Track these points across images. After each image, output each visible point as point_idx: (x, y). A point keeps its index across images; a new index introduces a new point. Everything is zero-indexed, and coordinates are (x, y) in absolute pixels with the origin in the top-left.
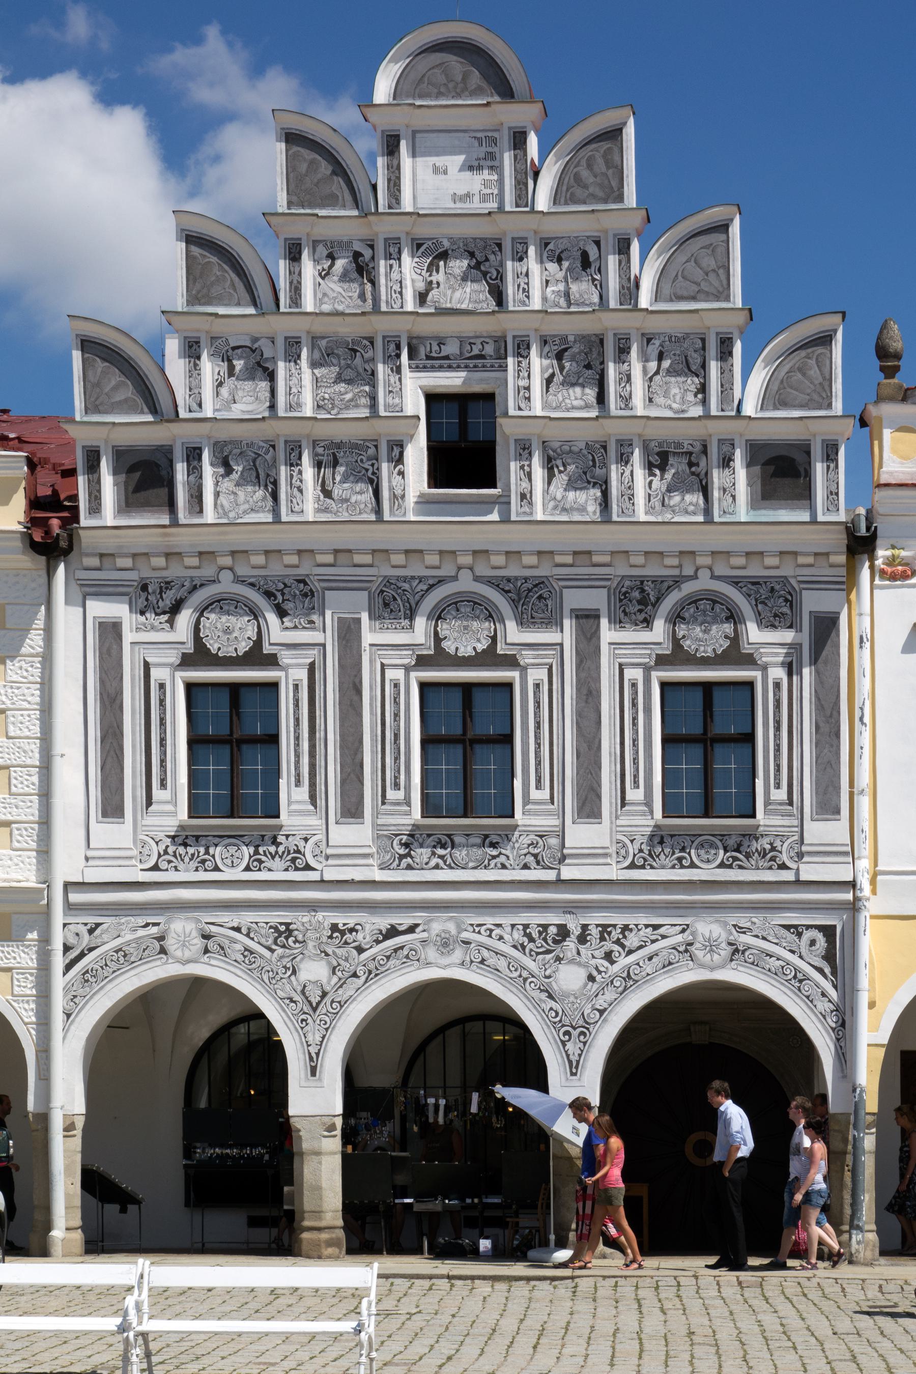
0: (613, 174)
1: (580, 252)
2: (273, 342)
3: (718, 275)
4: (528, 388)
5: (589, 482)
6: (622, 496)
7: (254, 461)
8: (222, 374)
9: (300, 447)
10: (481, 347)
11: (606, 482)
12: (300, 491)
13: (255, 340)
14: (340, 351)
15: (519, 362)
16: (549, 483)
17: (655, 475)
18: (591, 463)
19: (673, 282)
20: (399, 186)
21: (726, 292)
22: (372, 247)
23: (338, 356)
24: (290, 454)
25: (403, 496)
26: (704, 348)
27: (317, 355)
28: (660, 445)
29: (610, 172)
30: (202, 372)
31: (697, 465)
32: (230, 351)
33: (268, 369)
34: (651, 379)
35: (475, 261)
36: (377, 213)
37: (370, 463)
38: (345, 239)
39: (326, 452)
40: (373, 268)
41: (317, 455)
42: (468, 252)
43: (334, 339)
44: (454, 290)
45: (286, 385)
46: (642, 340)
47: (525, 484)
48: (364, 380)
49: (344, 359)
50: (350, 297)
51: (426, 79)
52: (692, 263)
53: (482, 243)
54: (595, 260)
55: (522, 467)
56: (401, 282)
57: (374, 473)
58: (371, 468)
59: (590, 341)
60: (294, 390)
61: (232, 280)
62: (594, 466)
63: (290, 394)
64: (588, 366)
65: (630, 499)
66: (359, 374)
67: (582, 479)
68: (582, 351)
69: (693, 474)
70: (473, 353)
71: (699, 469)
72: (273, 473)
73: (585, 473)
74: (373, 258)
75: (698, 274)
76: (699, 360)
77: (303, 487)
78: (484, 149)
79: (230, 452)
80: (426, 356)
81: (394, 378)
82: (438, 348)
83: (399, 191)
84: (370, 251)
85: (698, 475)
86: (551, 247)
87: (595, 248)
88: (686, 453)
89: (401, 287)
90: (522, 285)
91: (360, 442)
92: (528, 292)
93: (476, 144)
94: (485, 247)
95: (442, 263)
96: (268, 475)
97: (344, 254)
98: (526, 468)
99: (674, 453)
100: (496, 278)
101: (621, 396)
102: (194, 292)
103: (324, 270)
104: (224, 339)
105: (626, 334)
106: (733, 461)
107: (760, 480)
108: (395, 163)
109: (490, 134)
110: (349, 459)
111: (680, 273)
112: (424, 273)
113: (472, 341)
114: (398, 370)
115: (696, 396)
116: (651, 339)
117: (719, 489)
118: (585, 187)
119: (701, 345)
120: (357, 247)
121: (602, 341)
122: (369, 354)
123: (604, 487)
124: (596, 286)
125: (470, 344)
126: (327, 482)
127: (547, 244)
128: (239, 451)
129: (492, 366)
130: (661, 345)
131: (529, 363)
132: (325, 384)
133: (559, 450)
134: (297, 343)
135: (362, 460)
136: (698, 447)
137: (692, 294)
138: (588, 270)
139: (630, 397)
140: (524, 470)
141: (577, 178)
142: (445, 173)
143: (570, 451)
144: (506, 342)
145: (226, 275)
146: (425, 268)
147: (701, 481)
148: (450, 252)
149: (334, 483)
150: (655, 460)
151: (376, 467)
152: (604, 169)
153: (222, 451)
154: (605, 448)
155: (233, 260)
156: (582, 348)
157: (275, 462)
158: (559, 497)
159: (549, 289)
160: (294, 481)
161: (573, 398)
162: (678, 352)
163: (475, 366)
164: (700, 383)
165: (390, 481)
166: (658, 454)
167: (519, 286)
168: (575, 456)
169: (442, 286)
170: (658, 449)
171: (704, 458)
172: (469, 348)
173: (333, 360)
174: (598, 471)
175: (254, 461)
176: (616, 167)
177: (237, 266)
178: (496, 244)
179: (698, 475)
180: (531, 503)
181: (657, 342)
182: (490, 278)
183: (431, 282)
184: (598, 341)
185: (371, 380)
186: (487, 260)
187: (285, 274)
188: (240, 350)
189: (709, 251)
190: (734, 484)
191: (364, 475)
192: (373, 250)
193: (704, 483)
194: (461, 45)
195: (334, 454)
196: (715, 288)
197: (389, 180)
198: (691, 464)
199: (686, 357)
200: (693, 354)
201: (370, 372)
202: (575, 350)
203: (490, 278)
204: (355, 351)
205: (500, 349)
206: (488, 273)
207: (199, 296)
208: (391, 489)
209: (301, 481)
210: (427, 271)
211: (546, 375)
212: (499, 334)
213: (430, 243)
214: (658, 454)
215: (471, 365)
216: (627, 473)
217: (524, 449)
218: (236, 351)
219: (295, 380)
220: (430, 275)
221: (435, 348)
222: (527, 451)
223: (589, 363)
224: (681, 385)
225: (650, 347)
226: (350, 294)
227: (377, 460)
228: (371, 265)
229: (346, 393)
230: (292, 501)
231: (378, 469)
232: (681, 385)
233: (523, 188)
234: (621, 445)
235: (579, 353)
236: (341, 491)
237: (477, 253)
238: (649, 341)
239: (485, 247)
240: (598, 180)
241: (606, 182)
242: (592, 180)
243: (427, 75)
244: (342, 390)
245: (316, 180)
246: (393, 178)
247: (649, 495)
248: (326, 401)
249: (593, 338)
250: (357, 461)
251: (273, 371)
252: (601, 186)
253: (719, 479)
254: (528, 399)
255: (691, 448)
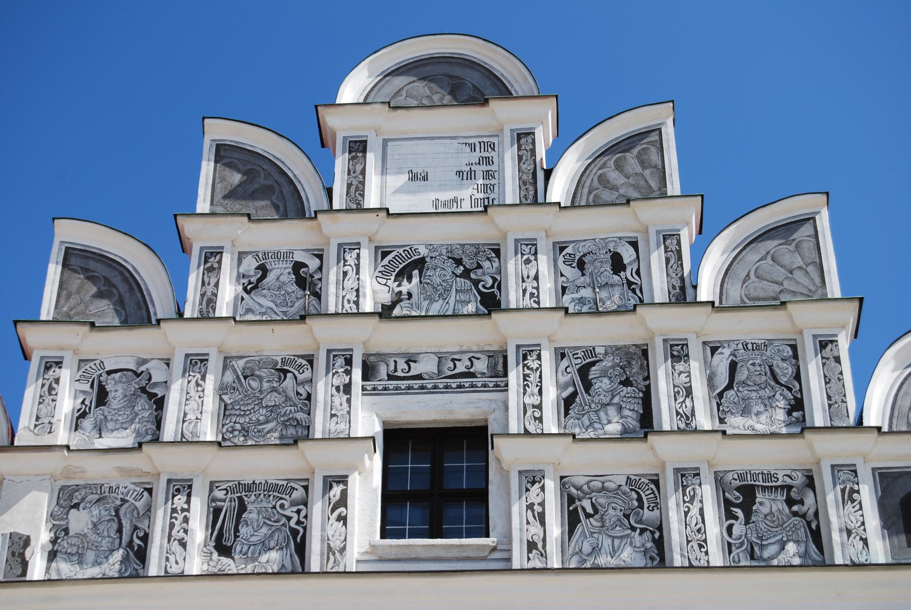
0: (652, 173)
1: (609, 255)
2: (168, 364)
3: (807, 273)
4: (539, 407)
5: (633, 529)
6: (688, 542)
7: (117, 511)
8: (87, 402)
9: (190, 487)
10: (469, 363)
11: (660, 528)
12: (183, 544)
13: (144, 362)
14: (263, 373)
15: (525, 376)
16: (571, 532)
17: (736, 518)
18: (636, 503)
19: (744, 283)
20: (363, 190)
21: (820, 292)
22: (320, 257)
23: (260, 378)
24: (174, 496)
25: (343, 550)
26: (796, 356)
27: (229, 377)
28: (741, 477)
29: (647, 172)
30: (59, 398)
31: (802, 502)
32: (105, 376)
33: (156, 395)
34: (720, 395)
35: (462, 268)
36: (331, 210)
37: (295, 509)
38: (284, 249)
39: (229, 495)
40: (320, 279)
41: (214, 500)
42: (453, 259)
43: (257, 358)
44: (432, 301)
45: (179, 410)
46: (704, 350)
47: (535, 529)
48: (295, 405)
49: (269, 381)
50: (284, 313)
51: (404, 93)
52: (769, 258)
53: (473, 249)
54: (631, 263)
55: (530, 507)
56: (357, 291)
57: (299, 523)
58: (295, 516)
59: (627, 353)
60: (191, 416)
61: (120, 295)
62: (641, 506)
63: (184, 421)
64: (627, 383)
65: (701, 546)
66: (288, 398)
67: (622, 525)
68: (618, 365)
69: (795, 514)
70: (456, 371)
71: (804, 509)
72: (144, 525)
73: (627, 517)
74: (320, 269)
75: (779, 273)
76: (790, 371)
77: (187, 539)
78: (477, 154)
79: (83, 499)
80: (388, 375)
81: (340, 399)
82: (406, 367)
83: (363, 196)
84: (317, 261)
85: (803, 516)
86: (569, 250)
87: (631, 250)
88: (782, 487)
89: (358, 296)
90: (530, 290)
91: (281, 483)
92: (538, 297)
93: (468, 149)
94: (477, 254)
95: (416, 272)
96: (136, 528)
97: (281, 265)
98: (537, 509)
99: (762, 486)
100: (492, 287)
101: (678, 413)
102: (65, 309)
103: (250, 283)
104: (97, 362)
105: (681, 340)
106: (858, 492)
107: (901, 519)
108: (359, 168)
109: (486, 140)
110: (264, 504)
111: (752, 273)
112: (390, 283)
113: (456, 357)
114: (347, 389)
115: (789, 413)
116: (717, 348)
117: (841, 530)
118: (614, 188)
119: (791, 353)
120: (299, 257)
121: (645, 353)
122: (307, 374)
123: (657, 535)
124: (634, 291)
125: (453, 360)
126: (226, 535)
127: (562, 249)
128: (97, 497)
129: (485, 386)
130: (733, 354)
131: (540, 377)
132: (238, 412)
133: (585, 488)
134: (202, 361)
135: (282, 506)
136: (799, 479)
137: (772, 294)
138: (622, 274)
139: (693, 414)
140: (533, 511)
141: (603, 181)
142: (425, 178)
143: (603, 489)
144: (505, 358)
145: (114, 290)
146: (393, 278)
147: (809, 524)
148: (428, 259)
149: (236, 537)
150: (735, 496)
151: (303, 514)
152: (639, 169)
153: (71, 497)
154: (656, 483)
155: (127, 274)
156: (618, 361)
157: (149, 510)
158: (587, 548)
159: (565, 296)
160: (174, 532)
161: (606, 422)
162: (757, 362)
163: (459, 387)
164: (795, 398)
165: (323, 529)
166: (738, 489)
167: (524, 291)
168: (610, 494)
169: (415, 297)
170: (738, 483)
171: (811, 494)
172: (452, 365)
173: (251, 381)
174: (647, 514)
175: (117, 511)
176: (655, 167)
177: (131, 280)
178: (493, 250)
179: (803, 516)
180: (543, 555)
181: (727, 352)
182: (484, 287)
183: (400, 292)
184: (640, 353)
185: (306, 405)
186: (479, 266)
187: (196, 286)
188: (120, 374)
189: (792, 247)
190: (863, 524)
191: (284, 525)
192: (321, 260)
193: (814, 526)
194: (452, 60)
195: (240, 498)
196: (804, 286)
197: (349, 186)
198: (790, 502)
199: (770, 367)
200: (780, 363)
201: (304, 395)
202: (607, 363)
203: (484, 287)
204: (285, 372)
205: (496, 365)
206: (480, 281)
207: (72, 313)
208: (325, 539)
209: (186, 531)
210: (395, 281)
211: (565, 394)
212: (495, 348)
213: (401, 251)
214: (738, 489)
215: (454, 386)
216: (695, 511)
217: (533, 483)
218: (113, 375)
219: (193, 404)
220: (399, 285)
221: (402, 365)
222: (537, 485)
223: (628, 379)
224: (766, 402)
225: (716, 357)
226: (285, 309)
227: (306, 505)
228: (317, 277)
229: (267, 422)
230: (167, 559)
231: (306, 517)
232: (766, 402)
233: (531, 188)
234: (683, 476)
235: (613, 367)
236: (245, 548)
237: (466, 261)
238: (714, 350)
239: (477, 254)
240: (631, 180)
241: (642, 183)
242: (622, 180)
243: (406, 88)
244: (261, 418)
245: (251, 191)
246: (355, 183)
247: (729, 544)
248: (236, 433)
249: (632, 350)
250: (274, 507)
251: (163, 397)
252: (636, 187)
253: (839, 517)
254: (540, 419)
255: (788, 481)
